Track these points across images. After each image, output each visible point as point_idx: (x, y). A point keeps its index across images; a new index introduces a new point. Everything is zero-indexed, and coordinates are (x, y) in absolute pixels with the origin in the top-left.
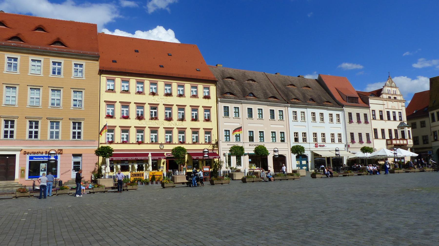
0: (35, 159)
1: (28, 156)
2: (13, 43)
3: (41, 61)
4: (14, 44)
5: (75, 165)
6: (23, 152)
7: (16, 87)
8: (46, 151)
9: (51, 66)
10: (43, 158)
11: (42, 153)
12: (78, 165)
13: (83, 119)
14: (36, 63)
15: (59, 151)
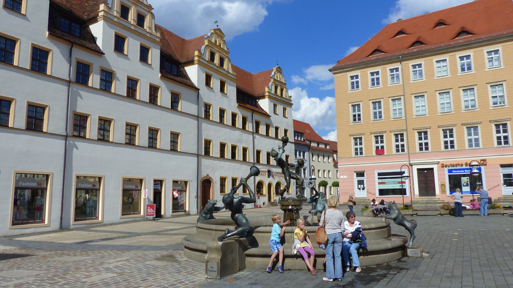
0: (455, 173)
1: (446, 170)
2: (415, 49)
3: (446, 60)
4: (416, 50)
5: (505, 179)
6: (440, 165)
7: (424, 95)
8: (466, 163)
9: (459, 62)
10: (463, 171)
11: (462, 165)
12: (509, 178)
13: (510, 119)
14: (442, 64)
15: (482, 162)
